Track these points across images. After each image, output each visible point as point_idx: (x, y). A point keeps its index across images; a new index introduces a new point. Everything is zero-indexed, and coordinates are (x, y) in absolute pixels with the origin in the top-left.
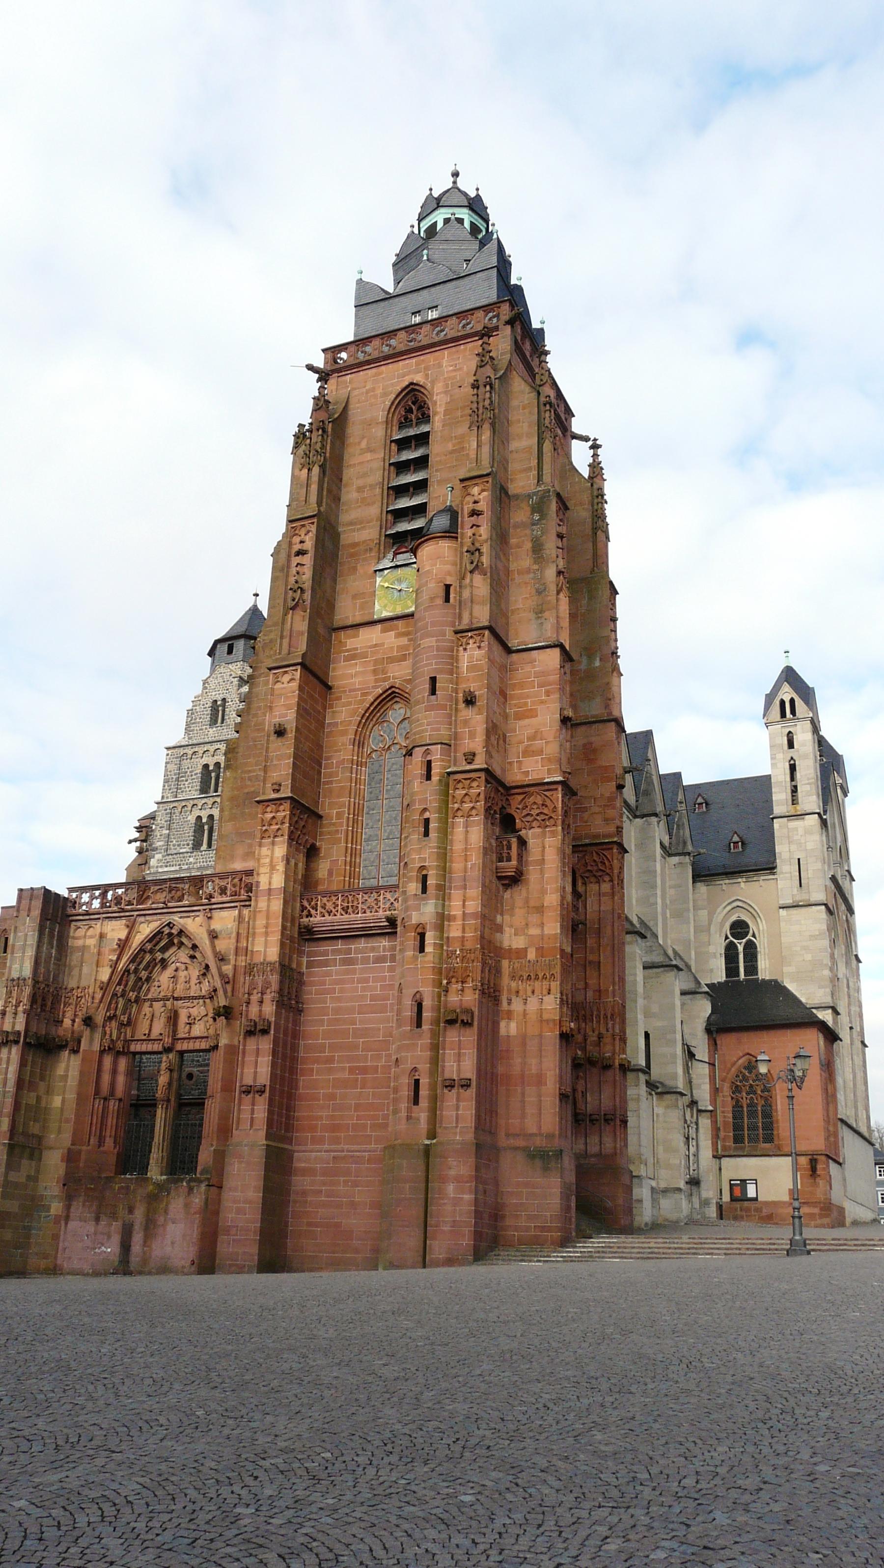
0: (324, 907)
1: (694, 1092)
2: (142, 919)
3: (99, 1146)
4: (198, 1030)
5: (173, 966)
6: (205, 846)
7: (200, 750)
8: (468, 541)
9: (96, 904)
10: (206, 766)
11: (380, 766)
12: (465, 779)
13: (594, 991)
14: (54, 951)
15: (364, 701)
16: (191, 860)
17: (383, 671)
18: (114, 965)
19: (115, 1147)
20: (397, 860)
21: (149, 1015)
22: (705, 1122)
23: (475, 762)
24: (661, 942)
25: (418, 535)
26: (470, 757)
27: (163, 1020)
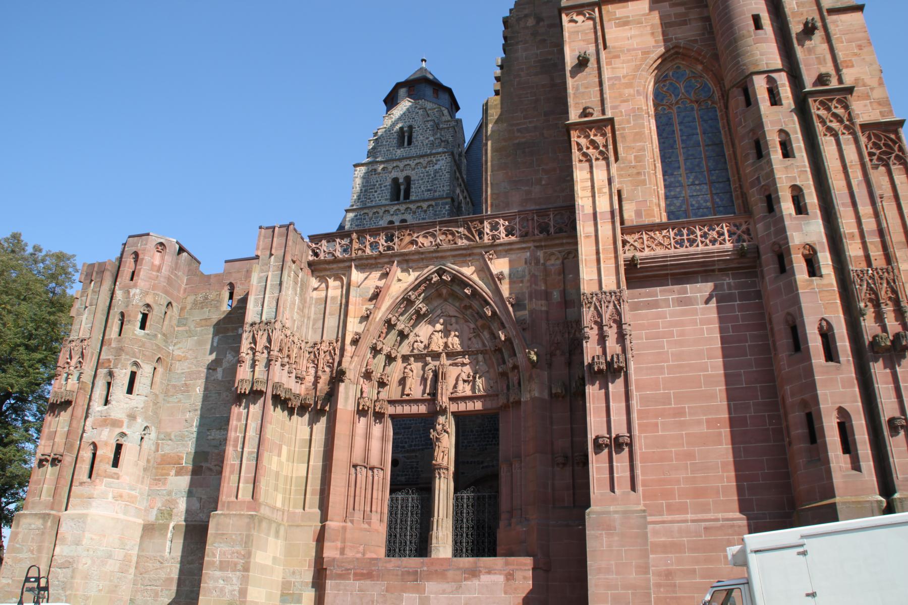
14: (297, 298)
15: (646, 59)
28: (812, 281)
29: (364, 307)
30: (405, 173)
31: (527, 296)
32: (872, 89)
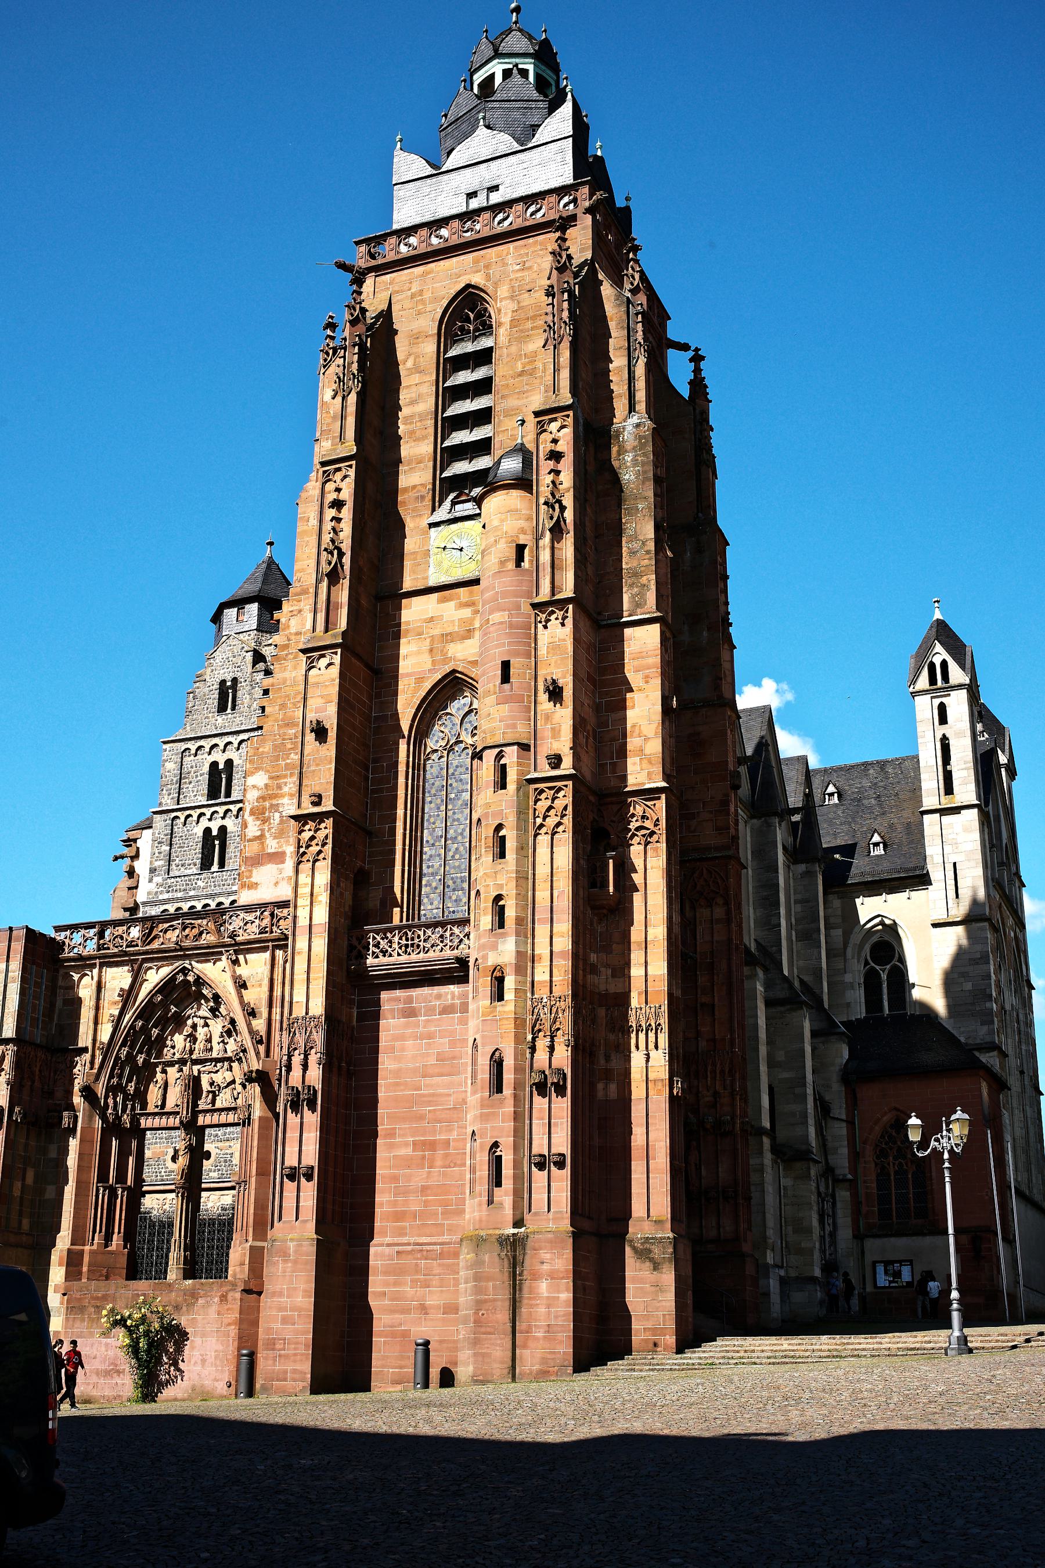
0: (377, 945)
1: (829, 1157)
2: (149, 965)
3: (106, 1246)
5: (189, 1022)
6: (215, 867)
7: (207, 744)
8: (545, 492)
9: (91, 947)
10: (214, 765)
11: (441, 769)
12: (550, 788)
13: (707, 1041)
16: (200, 883)
17: (442, 651)
18: (118, 1021)
19: (125, 1247)
20: (466, 885)
21: (161, 1083)
22: (843, 1195)
23: (562, 766)
24: (786, 973)
25: (480, 477)
26: (556, 761)
27: (178, 1089)
28: (496, 1007)
32: (647, 739)
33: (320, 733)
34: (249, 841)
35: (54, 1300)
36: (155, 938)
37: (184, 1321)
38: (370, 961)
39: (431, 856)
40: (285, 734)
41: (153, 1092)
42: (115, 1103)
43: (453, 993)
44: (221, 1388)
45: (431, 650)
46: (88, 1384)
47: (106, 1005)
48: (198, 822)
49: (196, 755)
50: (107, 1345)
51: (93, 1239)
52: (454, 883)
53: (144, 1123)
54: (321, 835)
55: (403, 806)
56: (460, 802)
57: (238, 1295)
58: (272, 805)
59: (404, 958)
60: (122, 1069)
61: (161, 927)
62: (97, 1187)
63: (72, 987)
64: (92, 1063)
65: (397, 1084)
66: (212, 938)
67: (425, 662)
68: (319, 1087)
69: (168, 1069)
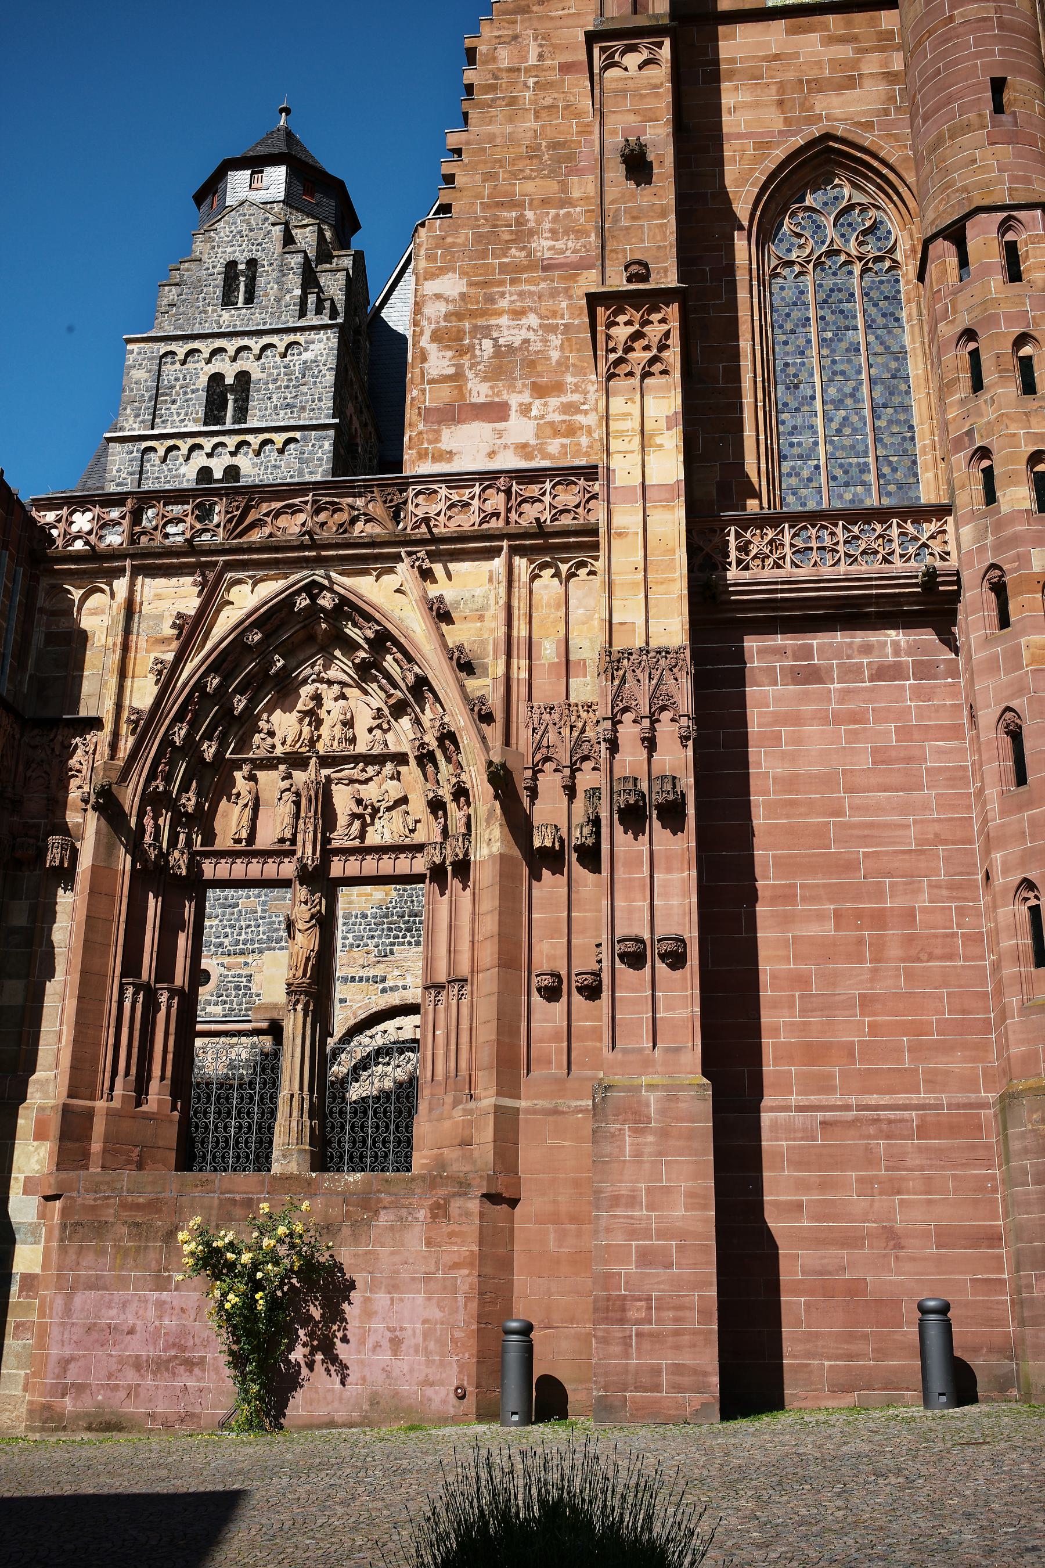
2: (240, 575)
3: (139, 1104)
4: (384, 831)
7: (206, 347)
10: (216, 379)
18: (167, 676)
19: (174, 1108)
29: (152, 656)
30: (240, 365)
31: (491, 647)
33: (637, 165)
34: (430, 382)
35: (22, 1208)
36: (253, 526)
37: (345, 1255)
38: (733, 574)
39: (795, 427)
40: (496, 218)
41: (226, 815)
42: (157, 827)
43: (896, 644)
44: (442, 1397)
45: (781, 103)
46: (116, 1388)
47: (143, 643)
48: (187, 459)
49: (184, 362)
50: (160, 1305)
51: (112, 1088)
52: (846, 472)
53: (209, 870)
54: (654, 332)
55: (749, 336)
56: (844, 345)
57: (474, 1205)
58: (475, 329)
59: (805, 572)
60: (173, 765)
61: (265, 507)
62: (121, 985)
63: (66, 611)
64: (114, 746)
65: (792, 803)
66: (378, 530)
67: (774, 120)
68: (688, 782)
69: (259, 774)
